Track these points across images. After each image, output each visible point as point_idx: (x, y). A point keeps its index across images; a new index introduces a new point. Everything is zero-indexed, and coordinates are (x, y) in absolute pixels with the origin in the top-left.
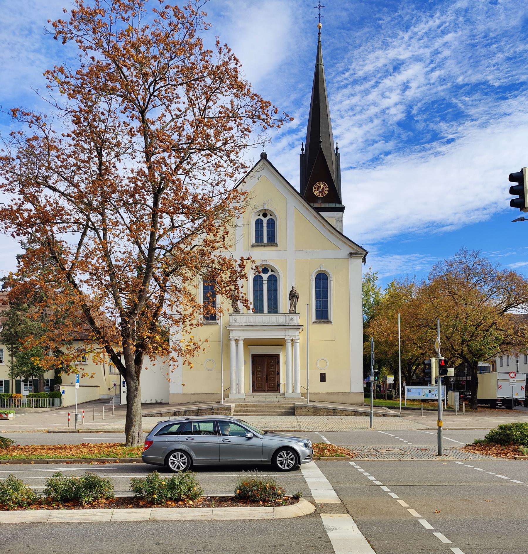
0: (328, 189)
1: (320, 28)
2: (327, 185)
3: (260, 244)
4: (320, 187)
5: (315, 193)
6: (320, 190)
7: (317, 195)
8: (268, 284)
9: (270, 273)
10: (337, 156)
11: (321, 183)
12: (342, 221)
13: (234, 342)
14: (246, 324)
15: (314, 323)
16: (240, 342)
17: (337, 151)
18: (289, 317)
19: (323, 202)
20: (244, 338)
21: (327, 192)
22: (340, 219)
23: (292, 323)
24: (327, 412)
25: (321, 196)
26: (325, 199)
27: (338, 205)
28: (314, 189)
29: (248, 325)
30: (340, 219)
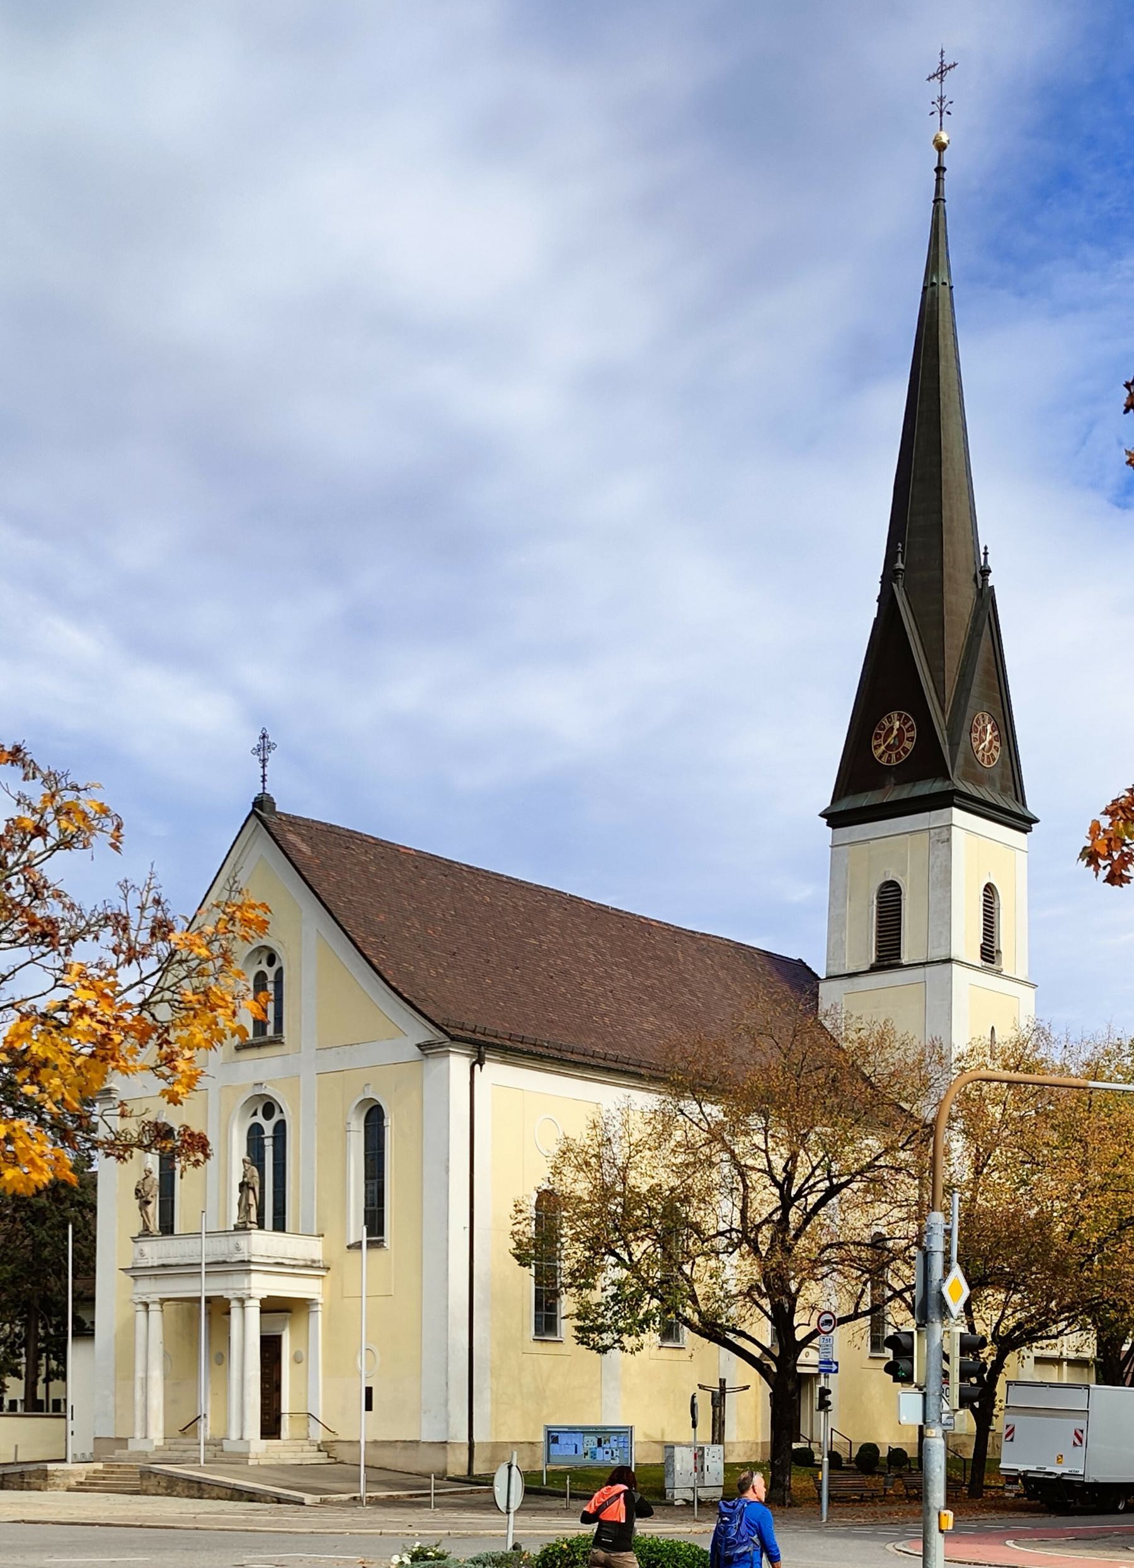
0: (914, 734)
1: (941, 147)
2: (912, 722)
3: (261, 1039)
4: (892, 729)
5: (877, 754)
6: (890, 740)
7: (883, 761)
8: (274, 1145)
9: (277, 1117)
10: (986, 600)
11: (894, 715)
12: (949, 840)
13: (141, 1307)
14: (161, 1262)
15: (349, 1247)
16: (151, 1307)
17: (985, 581)
18: (233, 1240)
19: (902, 781)
20: (156, 1297)
21: (910, 746)
22: (944, 836)
23: (239, 1257)
24: (189, 1488)
25: (894, 763)
26: (911, 770)
27: (936, 786)
28: (874, 743)
29: (164, 1266)
30: (944, 836)
